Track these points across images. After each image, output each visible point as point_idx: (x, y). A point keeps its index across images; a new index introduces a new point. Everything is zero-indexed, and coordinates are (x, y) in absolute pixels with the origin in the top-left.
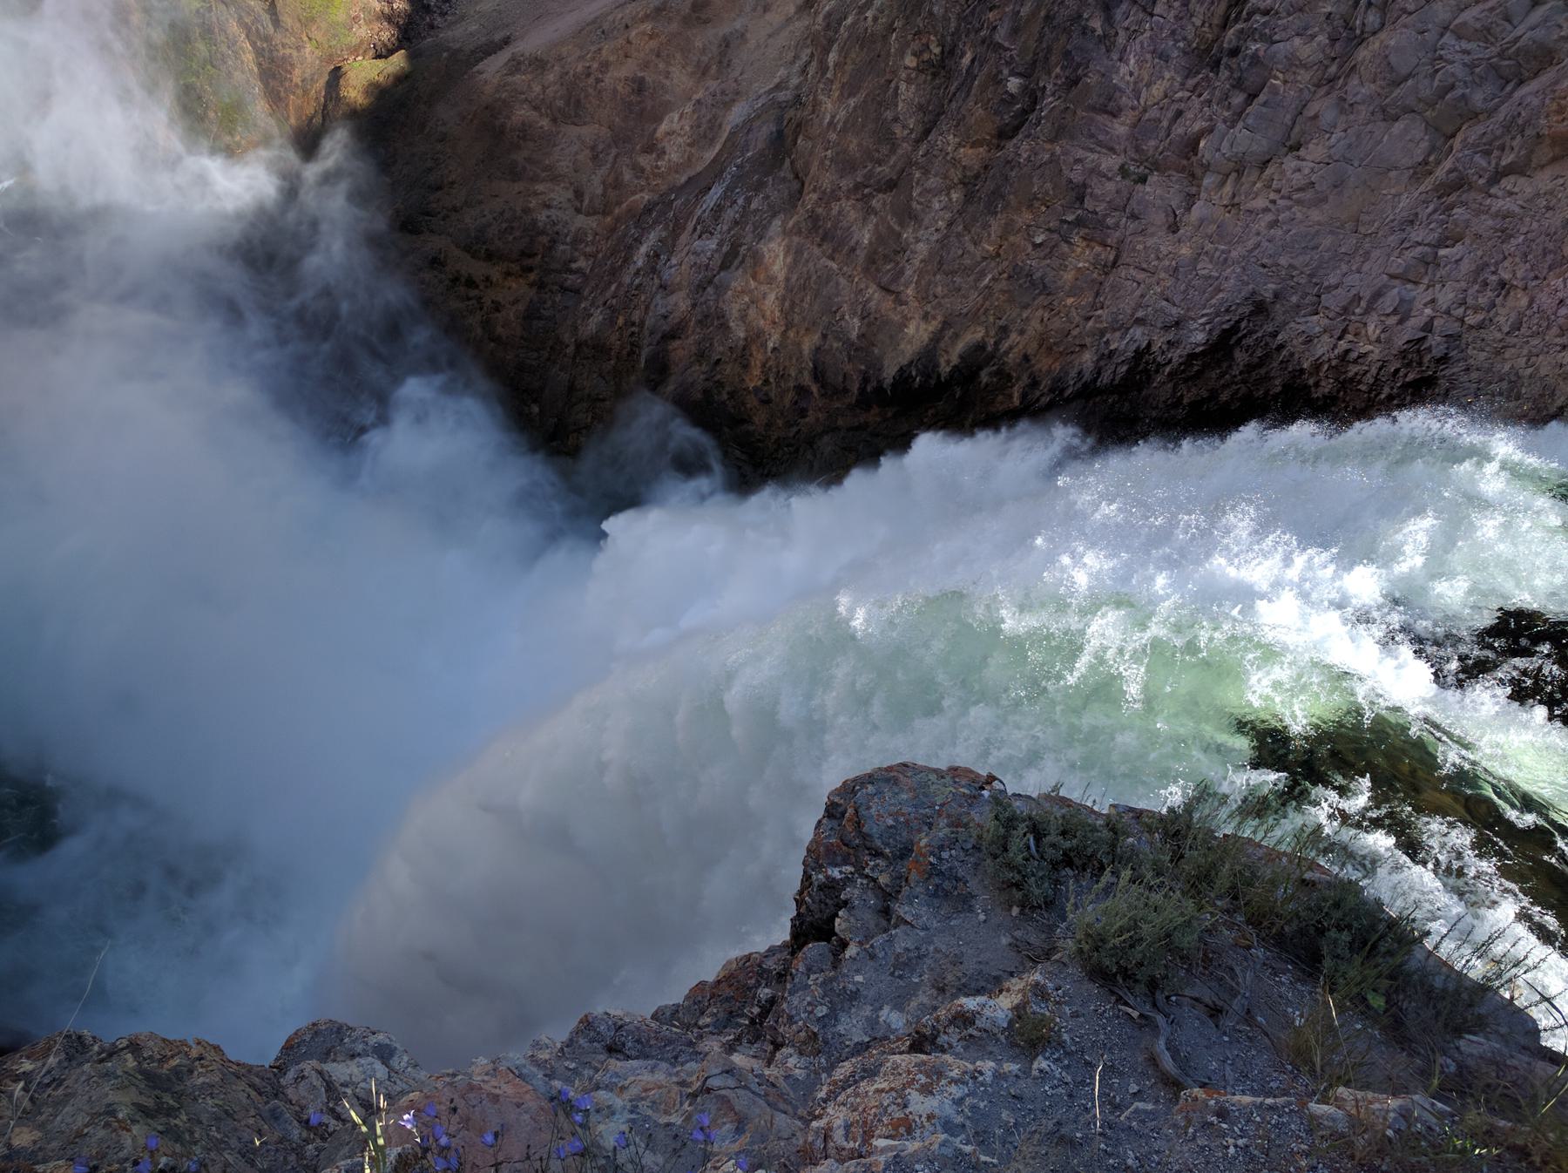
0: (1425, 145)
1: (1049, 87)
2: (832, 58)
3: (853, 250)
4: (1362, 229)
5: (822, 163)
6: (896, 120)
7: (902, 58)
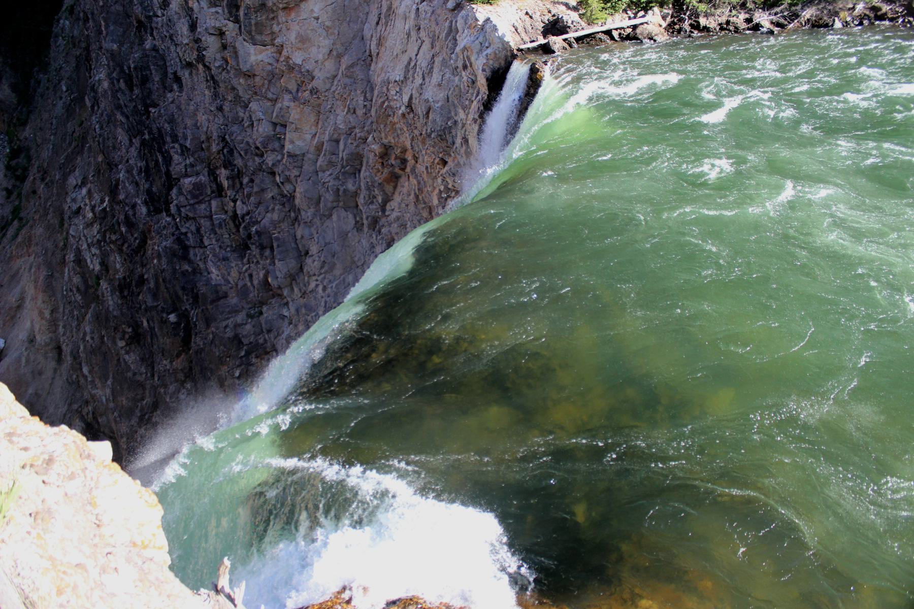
0: (350, 216)
1: (188, 307)
2: (85, 370)
4: (359, 264)
5: (116, 421)
6: (135, 374)
7: (116, 345)
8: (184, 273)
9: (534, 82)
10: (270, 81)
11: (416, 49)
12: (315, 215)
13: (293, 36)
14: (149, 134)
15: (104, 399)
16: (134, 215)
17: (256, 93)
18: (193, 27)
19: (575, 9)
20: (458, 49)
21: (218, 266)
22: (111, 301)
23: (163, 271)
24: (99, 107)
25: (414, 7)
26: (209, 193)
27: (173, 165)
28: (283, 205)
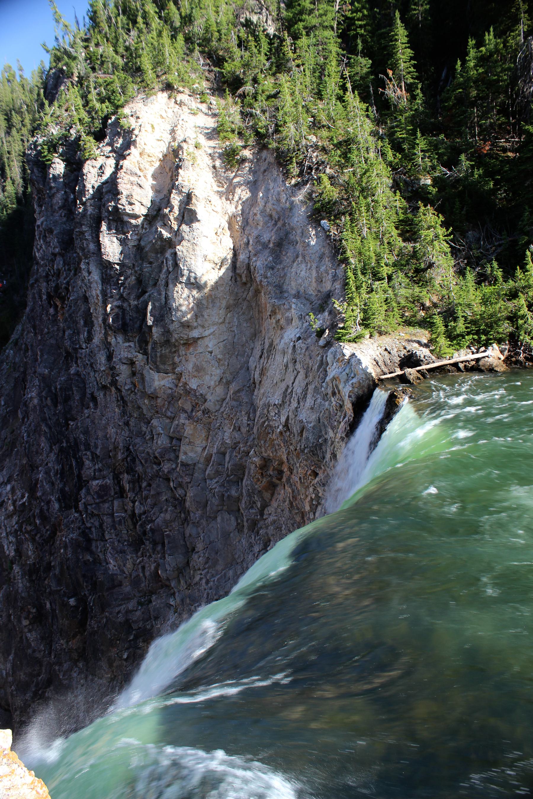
0: (233, 518)
1: (86, 593)
4: (239, 561)
6: (34, 651)
7: (21, 623)
8: (86, 563)
9: (391, 407)
10: (169, 403)
11: (293, 378)
12: (202, 517)
13: (190, 366)
14: (67, 442)
15: (4, 673)
16: (48, 510)
17: (157, 412)
18: (110, 357)
19: (426, 346)
20: (328, 379)
21: (116, 558)
22: (21, 584)
23: (68, 559)
24: (28, 419)
25: (292, 344)
26: (112, 494)
28: (175, 507)
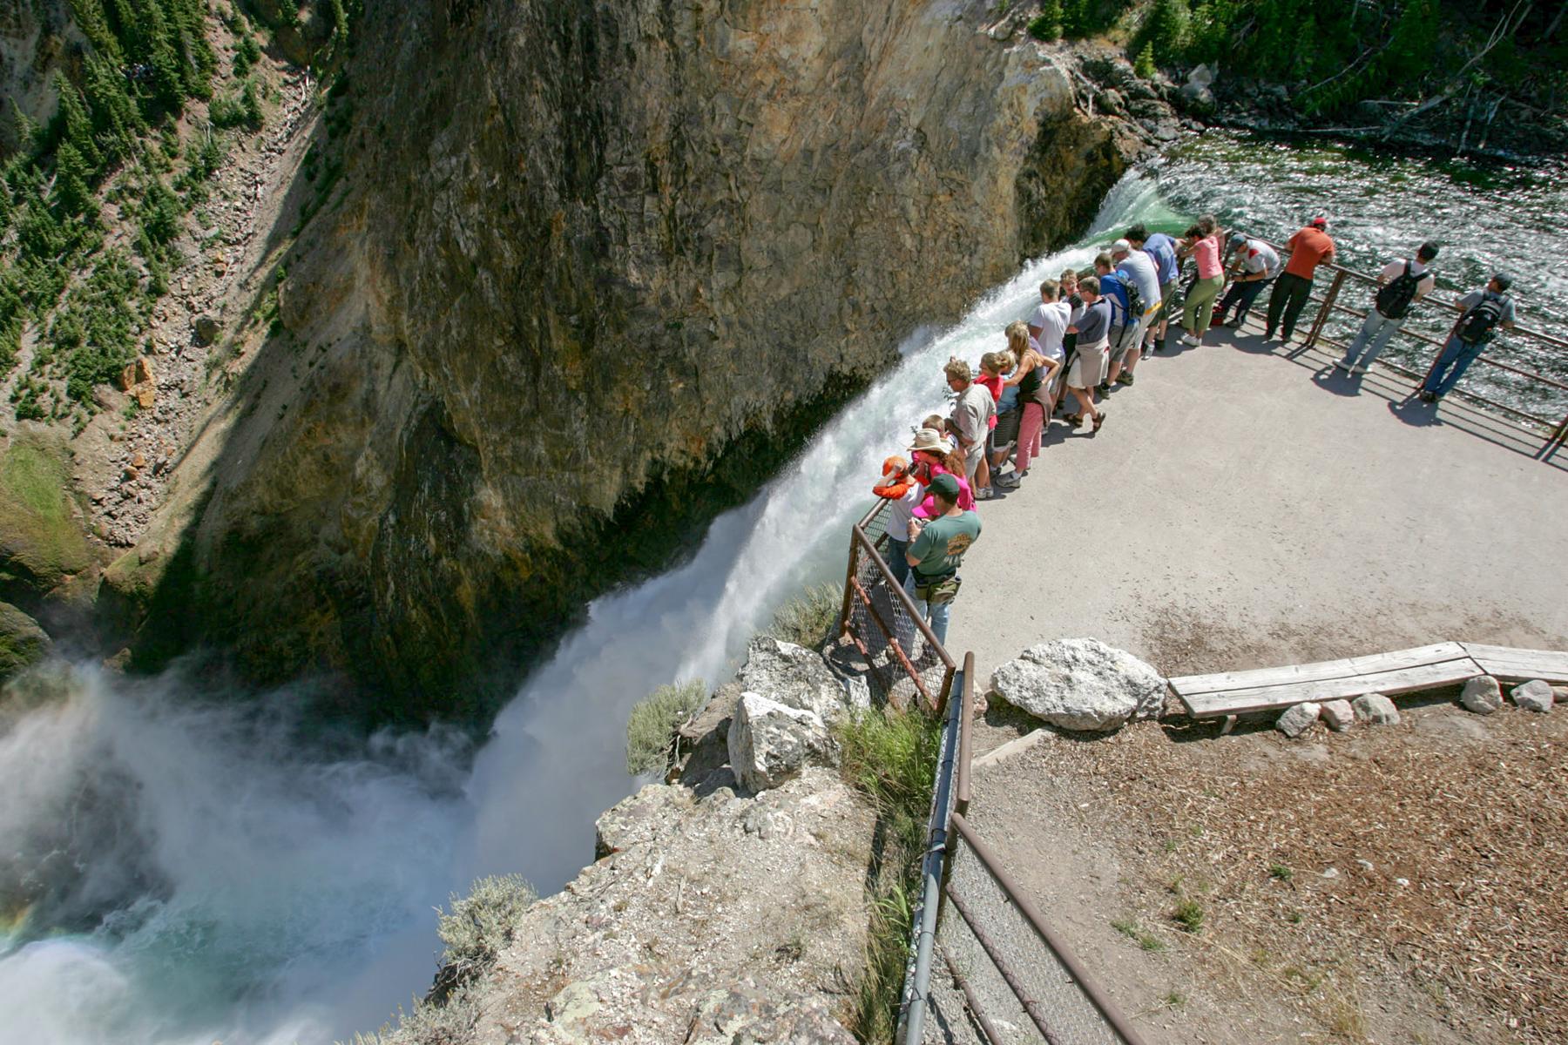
0: (809, 233)
3: (539, 463)
13: (784, 27)
24: (506, 65)
27: (609, 150)
